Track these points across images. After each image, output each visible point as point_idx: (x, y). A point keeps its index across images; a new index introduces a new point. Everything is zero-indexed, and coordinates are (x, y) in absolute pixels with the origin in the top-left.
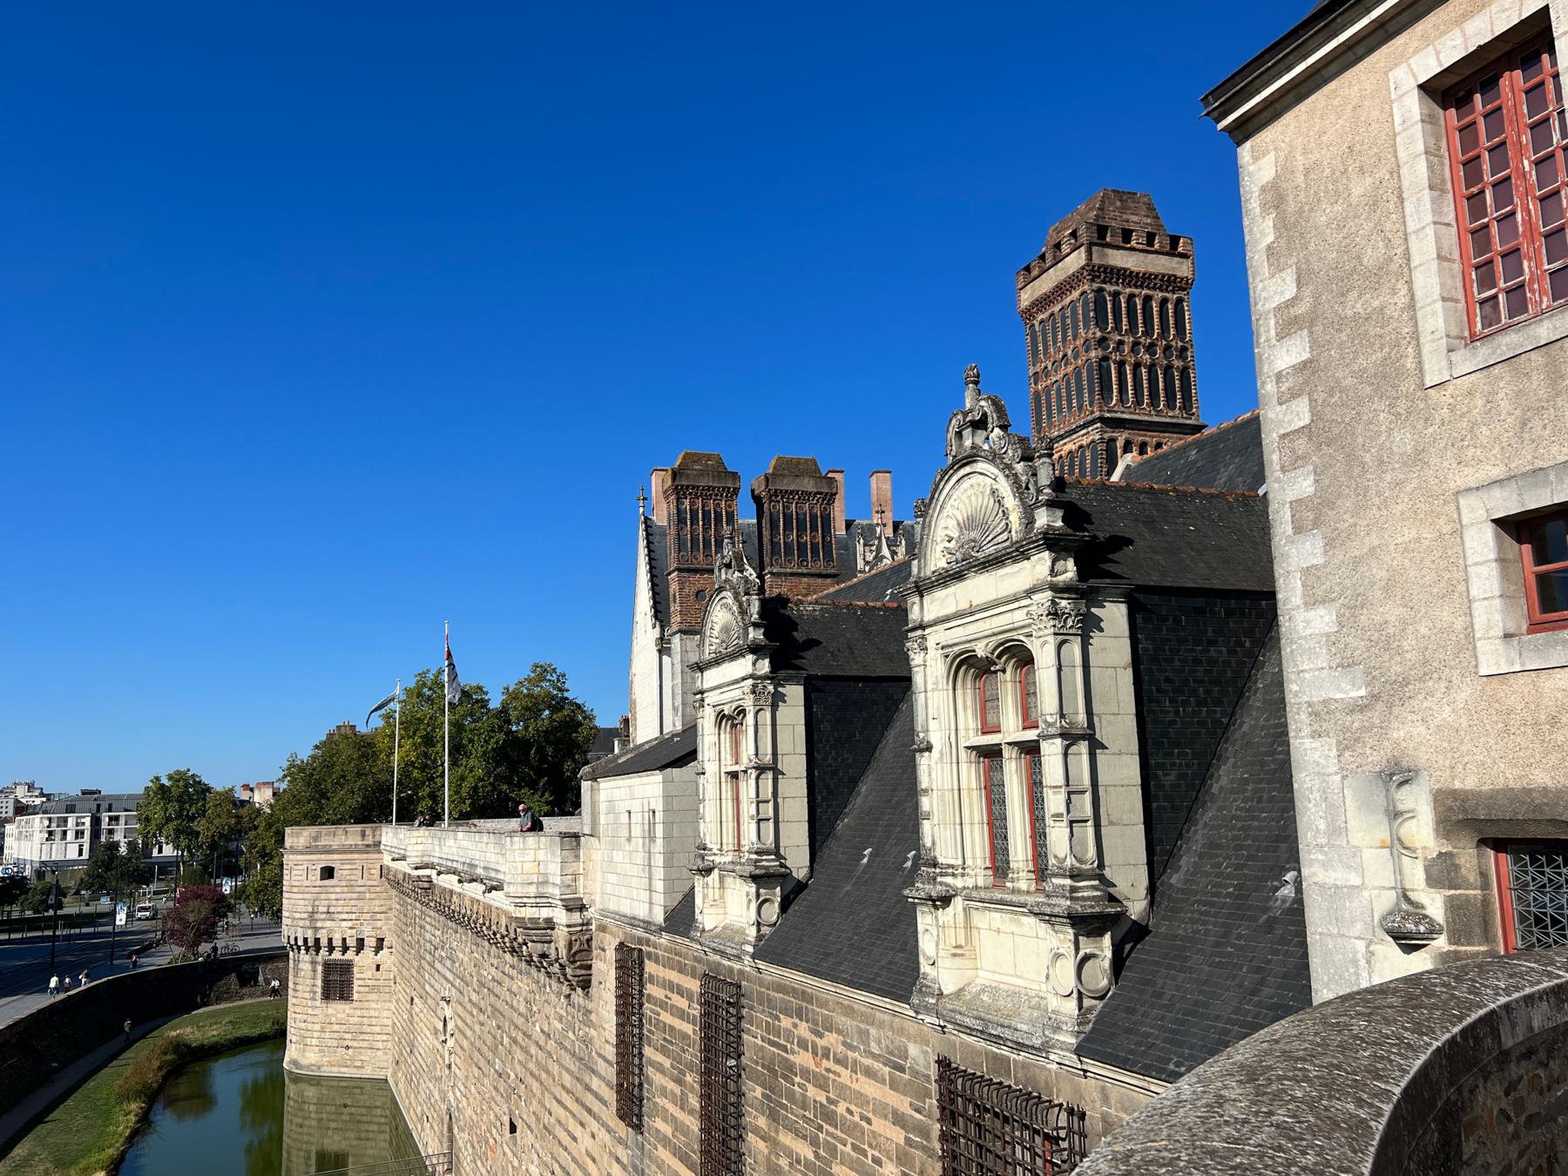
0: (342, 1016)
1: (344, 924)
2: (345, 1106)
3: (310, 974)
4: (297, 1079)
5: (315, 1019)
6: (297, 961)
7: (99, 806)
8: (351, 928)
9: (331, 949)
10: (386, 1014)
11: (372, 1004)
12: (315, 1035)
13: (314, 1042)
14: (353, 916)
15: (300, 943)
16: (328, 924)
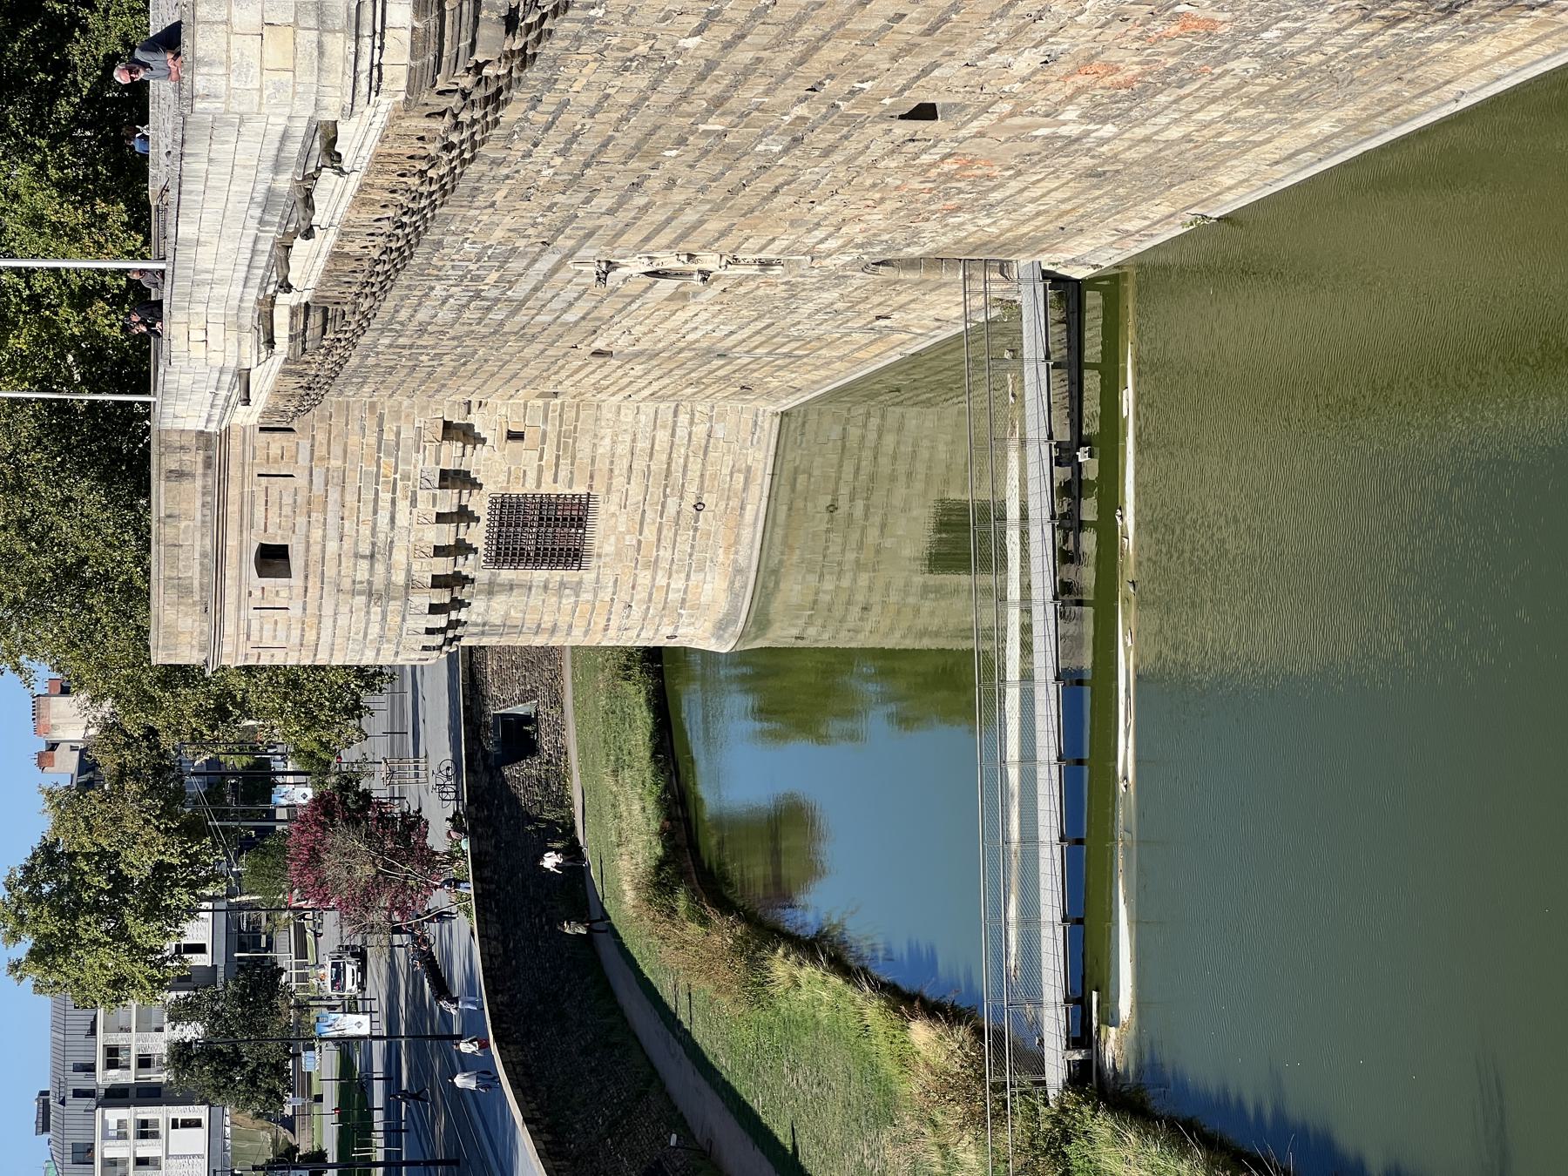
0: (623, 519)
1: (402, 519)
2: (832, 508)
3: (516, 597)
4: (760, 620)
5: (626, 582)
6: (485, 628)
7: (78, 1094)
8: (414, 503)
10: (627, 416)
11: (600, 450)
12: (661, 580)
13: (678, 583)
14: (385, 497)
15: (441, 621)
16: (399, 556)
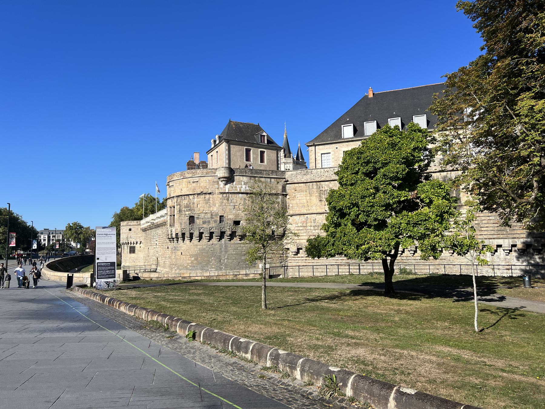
6: (124, 247)
7: (49, 233)
9: (131, 244)
15: (125, 243)
16: (130, 239)
